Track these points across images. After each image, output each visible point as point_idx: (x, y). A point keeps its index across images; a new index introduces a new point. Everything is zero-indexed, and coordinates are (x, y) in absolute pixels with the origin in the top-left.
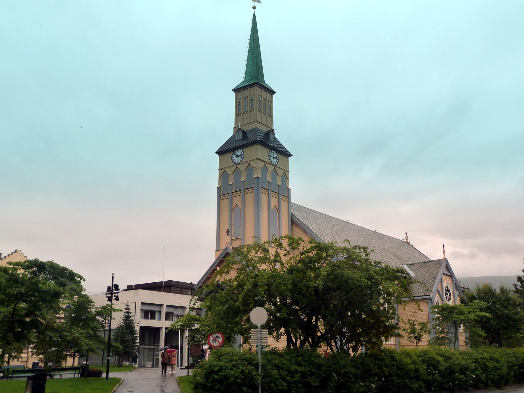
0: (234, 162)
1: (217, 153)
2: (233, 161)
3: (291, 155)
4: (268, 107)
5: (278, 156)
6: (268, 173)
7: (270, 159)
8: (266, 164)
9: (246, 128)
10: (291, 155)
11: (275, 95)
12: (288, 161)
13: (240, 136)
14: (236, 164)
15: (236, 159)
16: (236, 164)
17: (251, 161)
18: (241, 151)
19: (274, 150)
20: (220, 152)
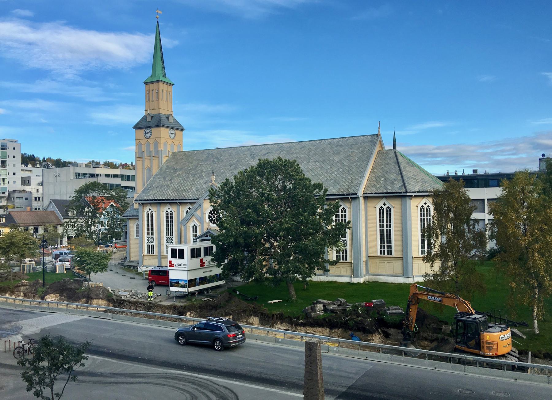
1: (133, 128)
6: (168, 145)
13: (149, 119)
16: (147, 138)
17: (157, 138)
18: (150, 130)
19: (172, 129)
20: (136, 127)
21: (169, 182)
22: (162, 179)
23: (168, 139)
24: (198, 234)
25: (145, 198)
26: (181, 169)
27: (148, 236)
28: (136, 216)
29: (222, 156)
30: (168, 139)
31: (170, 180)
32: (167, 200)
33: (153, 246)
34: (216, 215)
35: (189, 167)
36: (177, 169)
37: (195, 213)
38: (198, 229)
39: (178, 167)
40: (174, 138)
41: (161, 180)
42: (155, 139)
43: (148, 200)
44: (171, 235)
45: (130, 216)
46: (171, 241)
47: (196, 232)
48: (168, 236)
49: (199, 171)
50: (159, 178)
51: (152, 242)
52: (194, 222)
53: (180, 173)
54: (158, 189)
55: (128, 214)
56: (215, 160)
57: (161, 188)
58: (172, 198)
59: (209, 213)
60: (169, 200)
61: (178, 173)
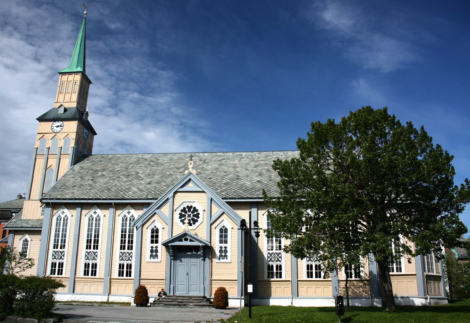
0: (53, 130)
2: (52, 129)
3: (96, 134)
4: (85, 92)
5: (88, 133)
7: (83, 134)
8: (81, 138)
9: (67, 105)
10: (96, 134)
11: (91, 85)
12: (93, 139)
13: (61, 111)
14: (55, 133)
15: (55, 128)
16: (55, 133)
17: (70, 133)
19: (87, 128)
21: (90, 182)
22: (80, 179)
23: (81, 137)
24: (161, 240)
25: (59, 197)
26: (104, 170)
27: (56, 250)
28: (26, 227)
29: (159, 160)
30: (81, 137)
31: (91, 180)
32: (96, 199)
33: (63, 264)
34: (192, 213)
35: (116, 169)
36: (97, 170)
37: (156, 211)
38: (160, 234)
39: (99, 168)
40: (86, 139)
41: (77, 180)
42: (67, 134)
43: (63, 199)
44: (94, 249)
45: (16, 227)
46: (94, 257)
47: (157, 236)
48: (88, 250)
49: (134, 173)
50: (73, 178)
51: (61, 258)
52: (158, 223)
53: (104, 173)
54: (76, 188)
55: (12, 225)
56: (152, 163)
57: (80, 187)
58: (104, 198)
59: (182, 211)
60: (100, 199)
61: (100, 173)
